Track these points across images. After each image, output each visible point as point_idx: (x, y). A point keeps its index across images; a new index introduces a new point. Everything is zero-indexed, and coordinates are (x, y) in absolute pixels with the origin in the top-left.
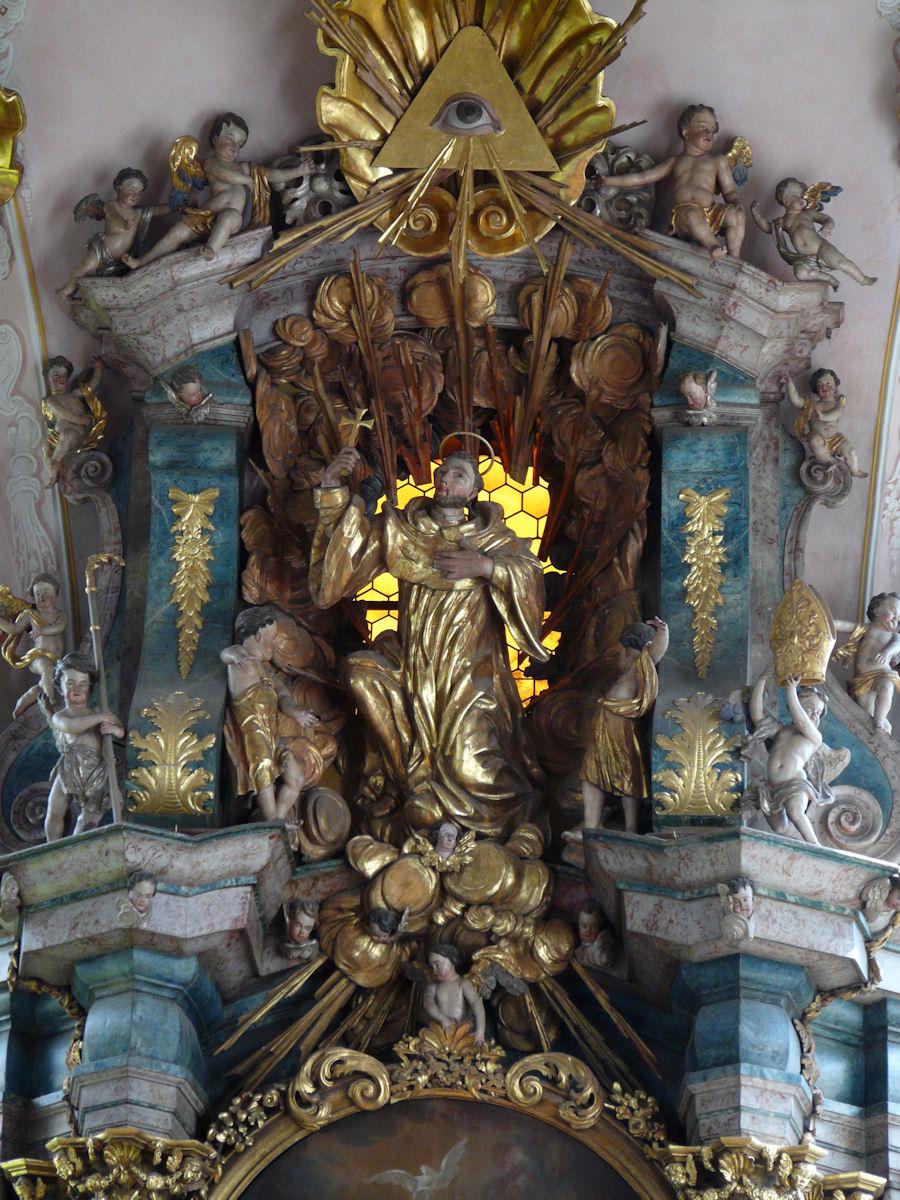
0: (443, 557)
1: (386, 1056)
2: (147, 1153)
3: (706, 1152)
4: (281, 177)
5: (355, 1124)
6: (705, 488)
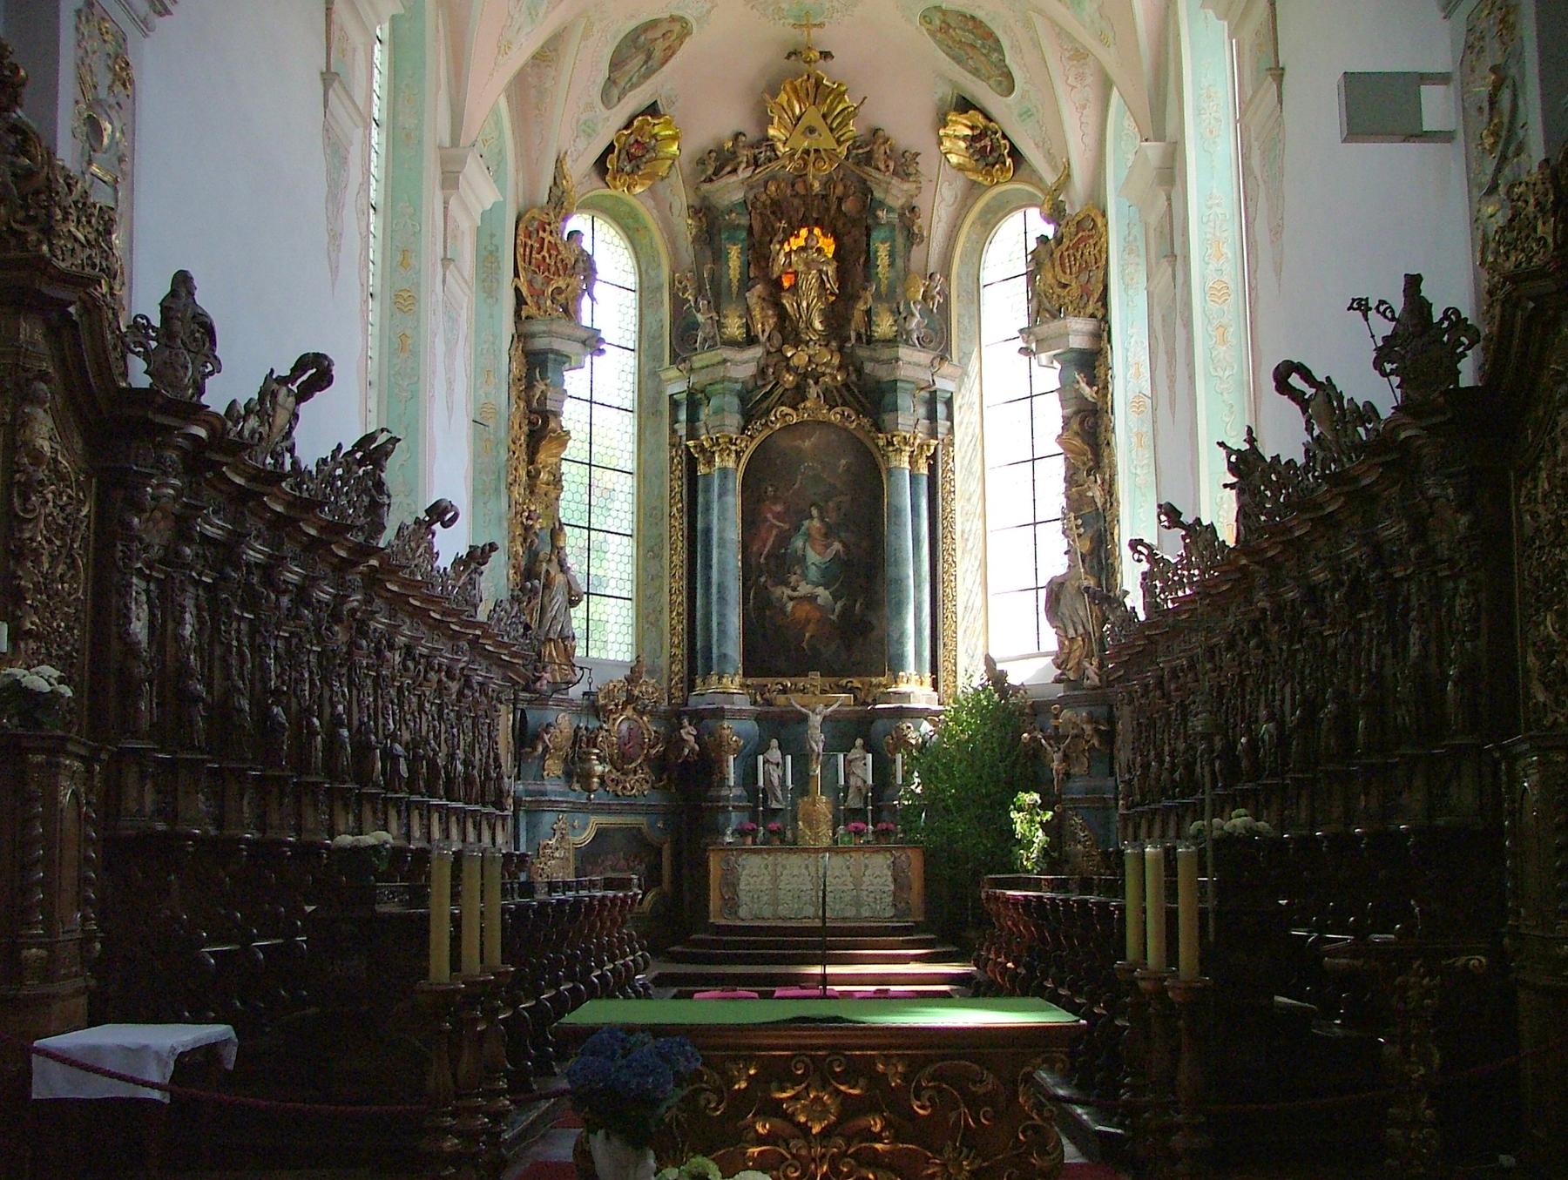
0: (808, 265)
1: (795, 408)
2: (731, 439)
3: (889, 437)
4: (757, 151)
5: (788, 428)
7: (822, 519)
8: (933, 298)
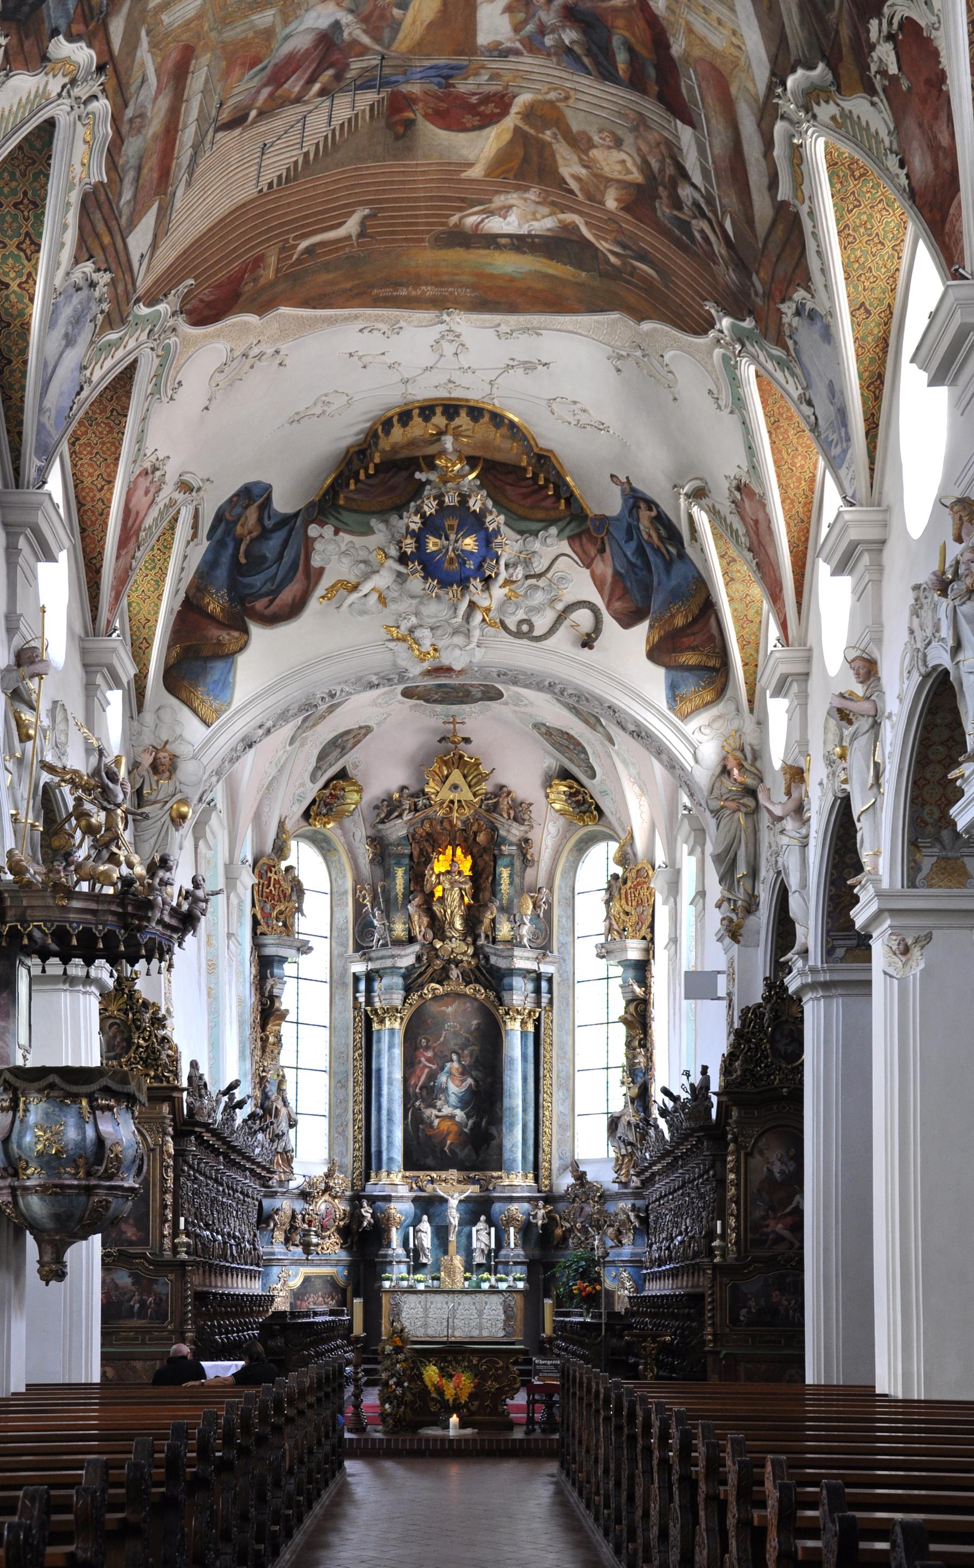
0: (451, 883)
1: (440, 982)
5: (436, 998)
6: (505, 867)
7: (459, 1062)
8: (540, 907)
